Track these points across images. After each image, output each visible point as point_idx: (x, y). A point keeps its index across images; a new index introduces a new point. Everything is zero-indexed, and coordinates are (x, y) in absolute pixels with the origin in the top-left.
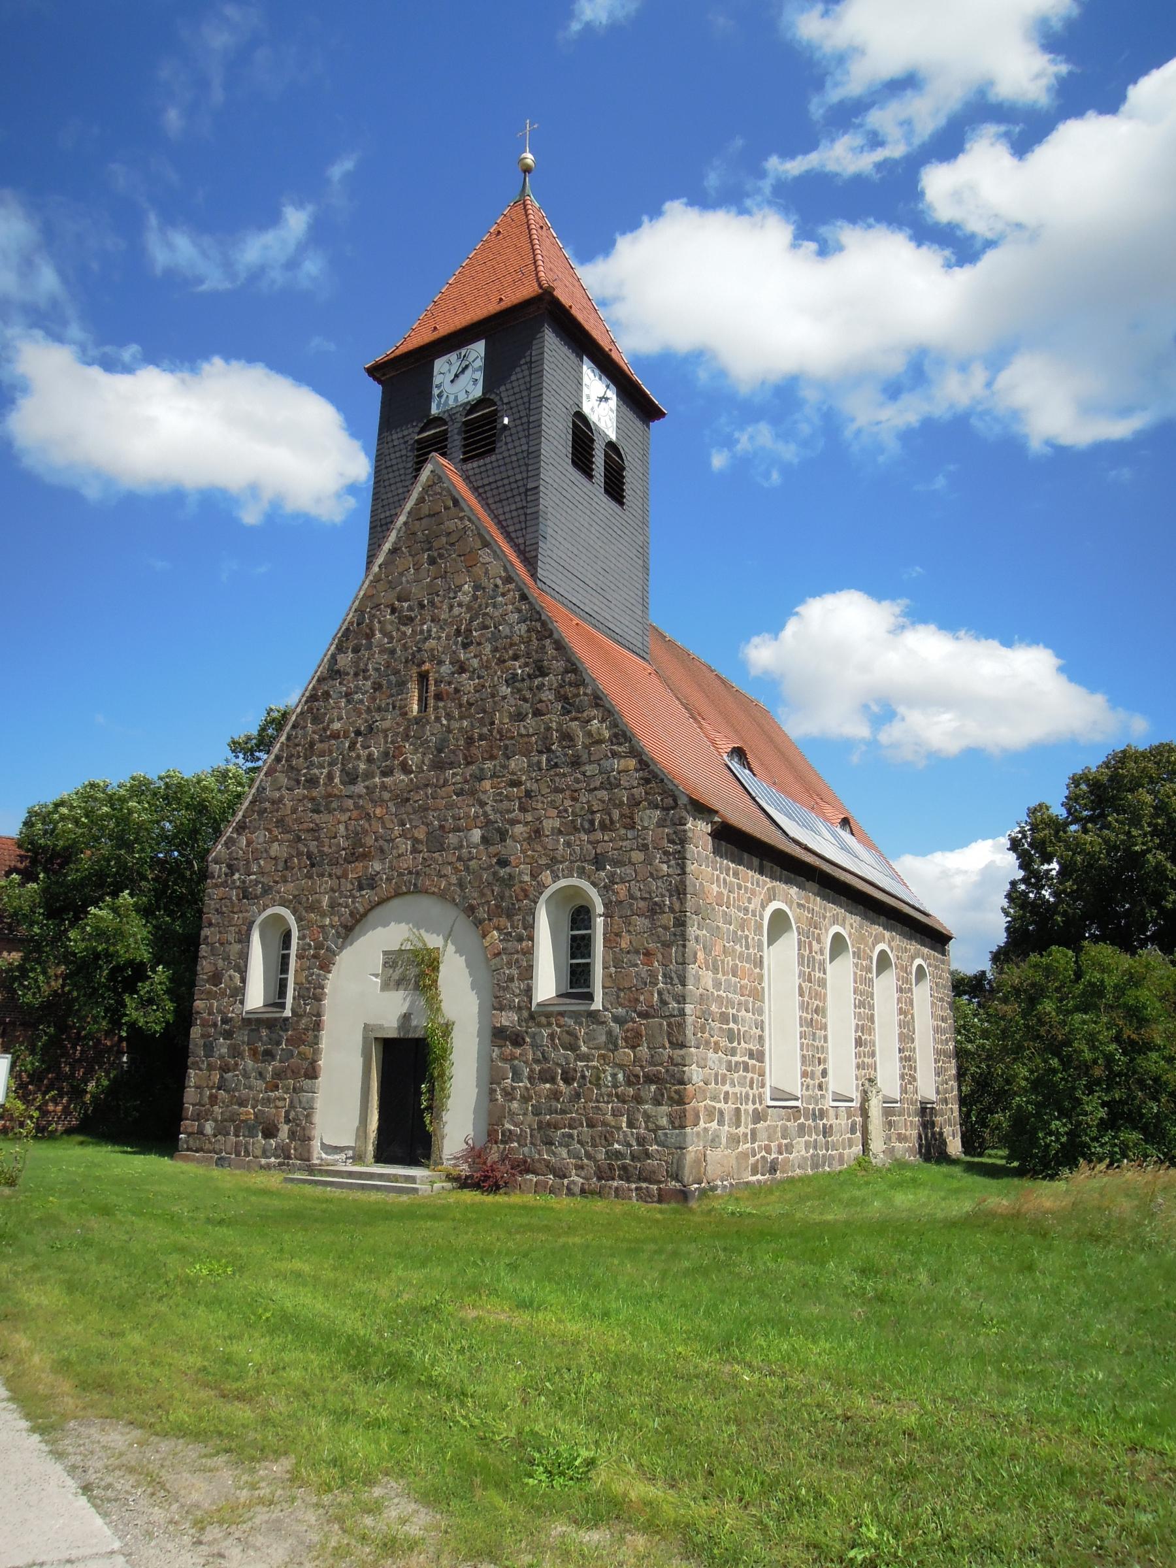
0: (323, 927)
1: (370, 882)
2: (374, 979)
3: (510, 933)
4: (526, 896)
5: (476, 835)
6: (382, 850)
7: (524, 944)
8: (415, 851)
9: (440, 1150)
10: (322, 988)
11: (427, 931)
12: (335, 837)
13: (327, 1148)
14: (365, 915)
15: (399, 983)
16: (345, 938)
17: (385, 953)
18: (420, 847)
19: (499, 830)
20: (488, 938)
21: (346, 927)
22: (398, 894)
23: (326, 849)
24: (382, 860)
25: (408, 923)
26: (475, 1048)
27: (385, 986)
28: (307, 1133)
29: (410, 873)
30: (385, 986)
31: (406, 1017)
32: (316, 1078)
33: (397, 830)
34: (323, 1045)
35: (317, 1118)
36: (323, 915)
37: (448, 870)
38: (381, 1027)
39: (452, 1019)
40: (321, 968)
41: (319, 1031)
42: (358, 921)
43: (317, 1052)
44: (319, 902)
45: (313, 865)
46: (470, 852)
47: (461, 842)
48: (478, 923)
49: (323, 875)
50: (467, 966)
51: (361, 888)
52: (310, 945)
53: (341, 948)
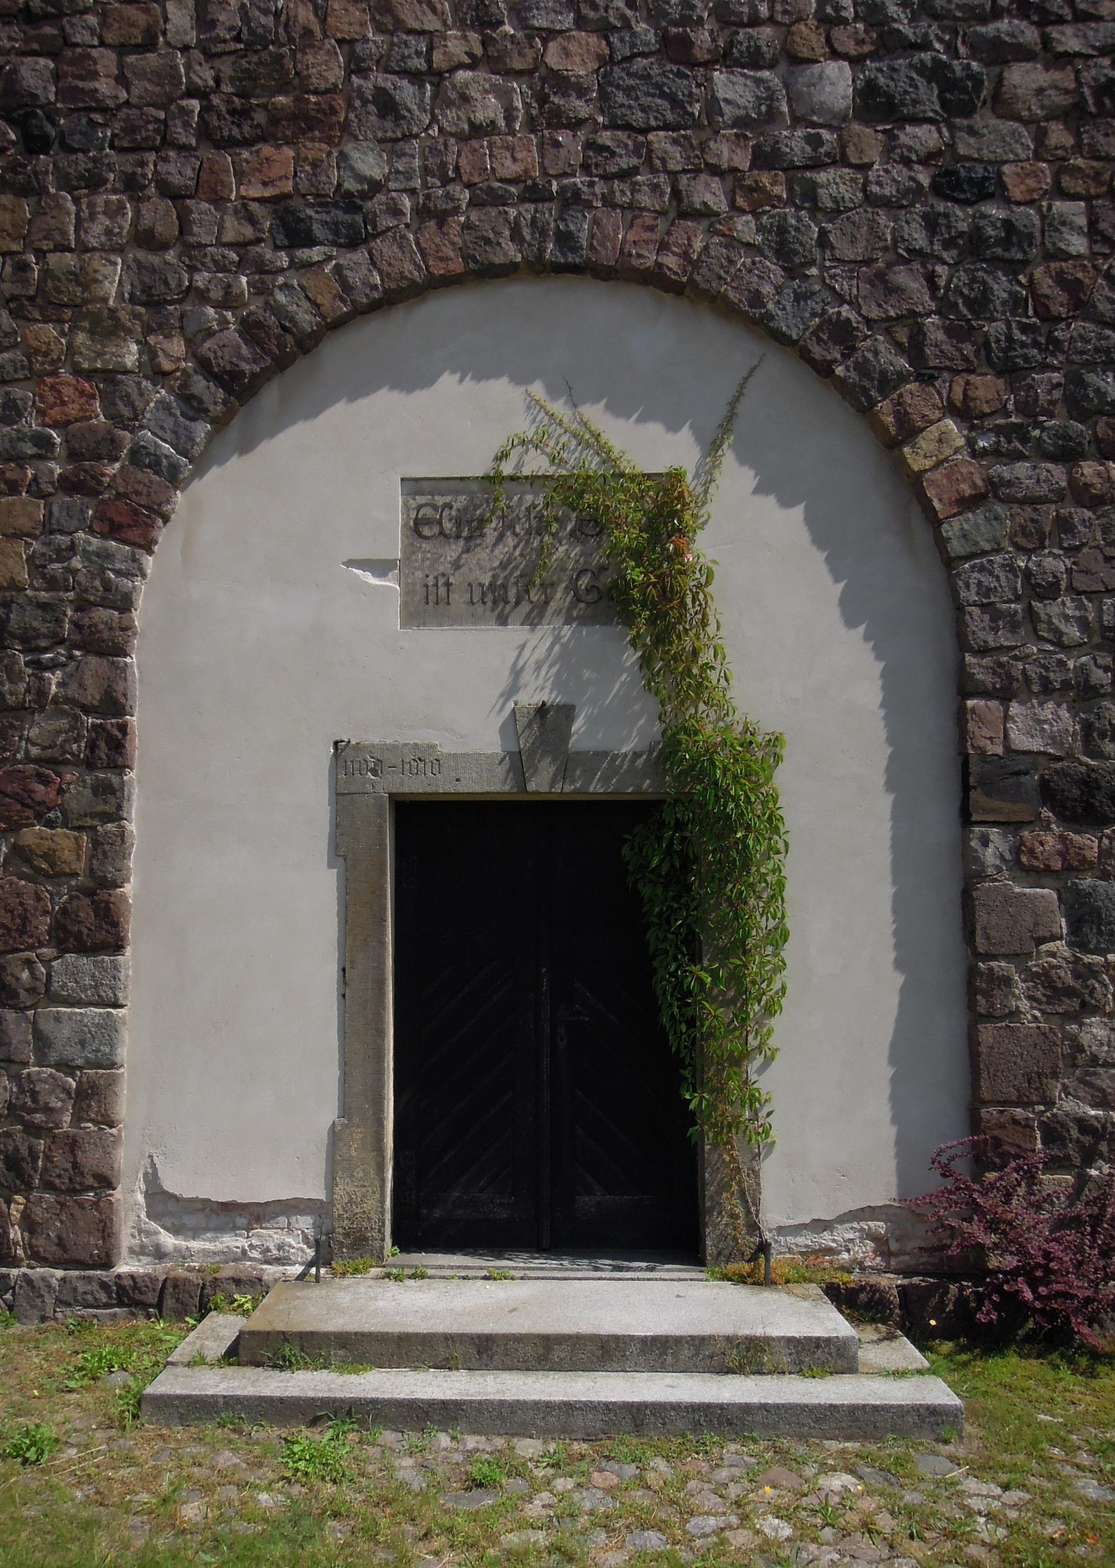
0: (110, 376)
1: (354, 218)
3: (1020, 432)
4: (1081, 306)
5: (836, 83)
6: (387, 105)
7: (1088, 469)
8: (548, 119)
9: (750, 1199)
10: (125, 604)
12: (148, 45)
13: (164, 1205)
14: (308, 344)
15: (499, 601)
16: (220, 424)
17: (413, 486)
18: (581, 108)
19: (937, 73)
20: (926, 442)
22: (485, 273)
23: (104, 87)
24: (392, 145)
25: (521, 378)
27: (428, 604)
29: (535, 194)
30: (428, 604)
31: (550, 721)
32: (117, 946)
33: (457, 45)
35: (129, 1103)
36: (107, 328)
37: (710, 193)
38: (424, 758)
39: (766, 722)
40: (114, 530)
41: (120, 767)
42: (282, 363)
43: (108, 849)
44: (84, 279)
45: (35, 144)
46: (815, 141)
47: (771, 98)
48: (861, 395)
49: (95, 183)
50: (819, 540)
51: (296, 235)
52: (43, 442)
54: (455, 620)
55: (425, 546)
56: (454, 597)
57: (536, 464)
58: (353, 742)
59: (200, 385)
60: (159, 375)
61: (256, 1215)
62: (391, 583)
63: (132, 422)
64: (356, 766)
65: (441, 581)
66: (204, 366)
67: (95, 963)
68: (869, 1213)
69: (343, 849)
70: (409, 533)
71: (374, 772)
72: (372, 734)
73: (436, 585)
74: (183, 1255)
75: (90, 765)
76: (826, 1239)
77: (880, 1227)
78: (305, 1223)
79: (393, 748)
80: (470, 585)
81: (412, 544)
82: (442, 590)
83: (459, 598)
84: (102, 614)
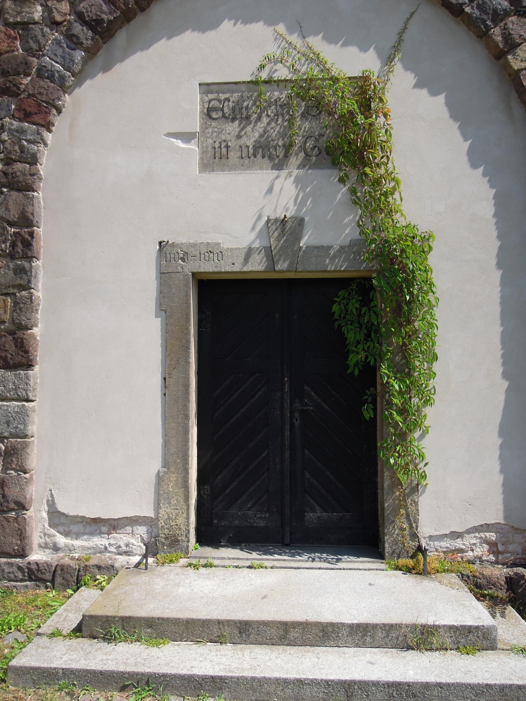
0: (25, 26)
2: (180, 144)
9: (412, 520)
10: (33, 160)
11: (330, 39)
16: (91, 53)
17: (206, 88)
21: (94, 25)
25: (271, 22)
26: (496, 292)
27: (216, 158)
28: (12, 492)
30: (216, 158)
32: (29, 365)
34: (40, 292)
35: (36, 458)
38: (212, 251)
39: (423, 227)
40: (27, 116)
41: (30, 258)
50: (454, 115)
53: (80, 77)
54: (232, 168)
55: (214, 124)
56: (231, 154)
57: (282, 73)
58: (170, 242)
59: (78, 28)
60: (55, 24)
61: (113, 525)
62: (193, 146)
63: (37, 52)
64: (172, 256)
65: (223, 145)
66: (80, 17)
67: (15, 375)
68: (487, 527)
69: (165, 306)
70: (204, 116)
71: (183, 260)
72: (181, 236)
73: (220, 147)
74: (71, 549)
75: (12, 256)
76: (459, 543)
77: (492, 536)
78: (142, 530)
79: (194, 245)
80: (241, 147)
81: (206, 123)
82: (224, 150)
83: (234, 155)
84: (19, 166)
